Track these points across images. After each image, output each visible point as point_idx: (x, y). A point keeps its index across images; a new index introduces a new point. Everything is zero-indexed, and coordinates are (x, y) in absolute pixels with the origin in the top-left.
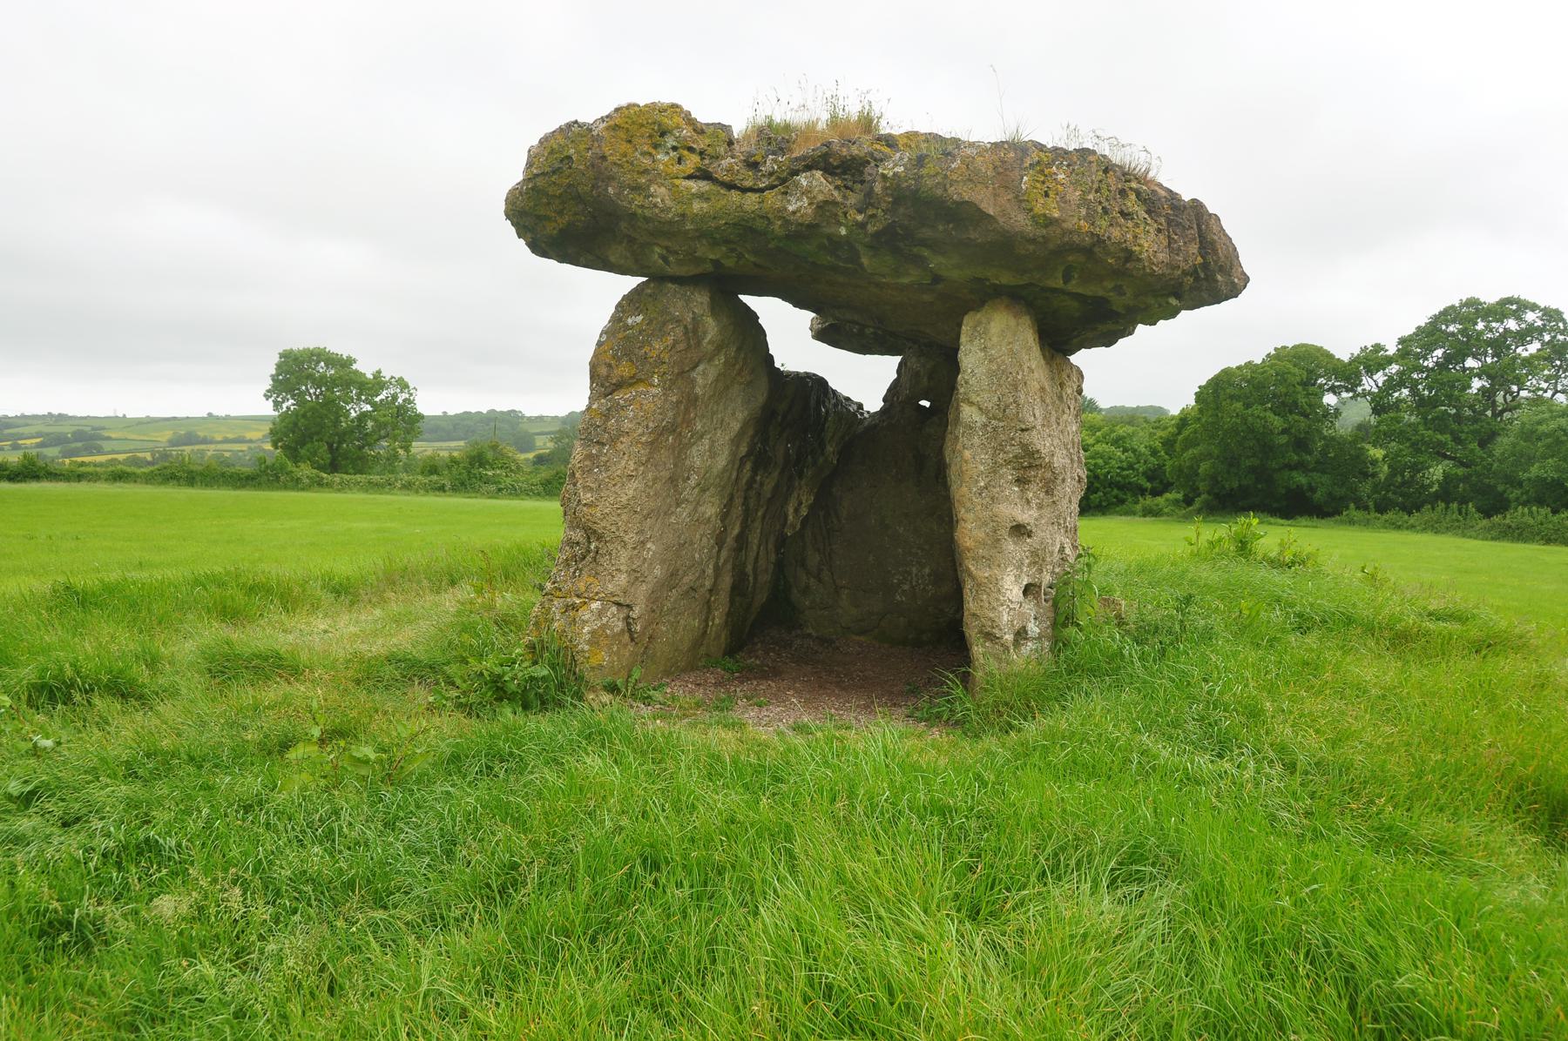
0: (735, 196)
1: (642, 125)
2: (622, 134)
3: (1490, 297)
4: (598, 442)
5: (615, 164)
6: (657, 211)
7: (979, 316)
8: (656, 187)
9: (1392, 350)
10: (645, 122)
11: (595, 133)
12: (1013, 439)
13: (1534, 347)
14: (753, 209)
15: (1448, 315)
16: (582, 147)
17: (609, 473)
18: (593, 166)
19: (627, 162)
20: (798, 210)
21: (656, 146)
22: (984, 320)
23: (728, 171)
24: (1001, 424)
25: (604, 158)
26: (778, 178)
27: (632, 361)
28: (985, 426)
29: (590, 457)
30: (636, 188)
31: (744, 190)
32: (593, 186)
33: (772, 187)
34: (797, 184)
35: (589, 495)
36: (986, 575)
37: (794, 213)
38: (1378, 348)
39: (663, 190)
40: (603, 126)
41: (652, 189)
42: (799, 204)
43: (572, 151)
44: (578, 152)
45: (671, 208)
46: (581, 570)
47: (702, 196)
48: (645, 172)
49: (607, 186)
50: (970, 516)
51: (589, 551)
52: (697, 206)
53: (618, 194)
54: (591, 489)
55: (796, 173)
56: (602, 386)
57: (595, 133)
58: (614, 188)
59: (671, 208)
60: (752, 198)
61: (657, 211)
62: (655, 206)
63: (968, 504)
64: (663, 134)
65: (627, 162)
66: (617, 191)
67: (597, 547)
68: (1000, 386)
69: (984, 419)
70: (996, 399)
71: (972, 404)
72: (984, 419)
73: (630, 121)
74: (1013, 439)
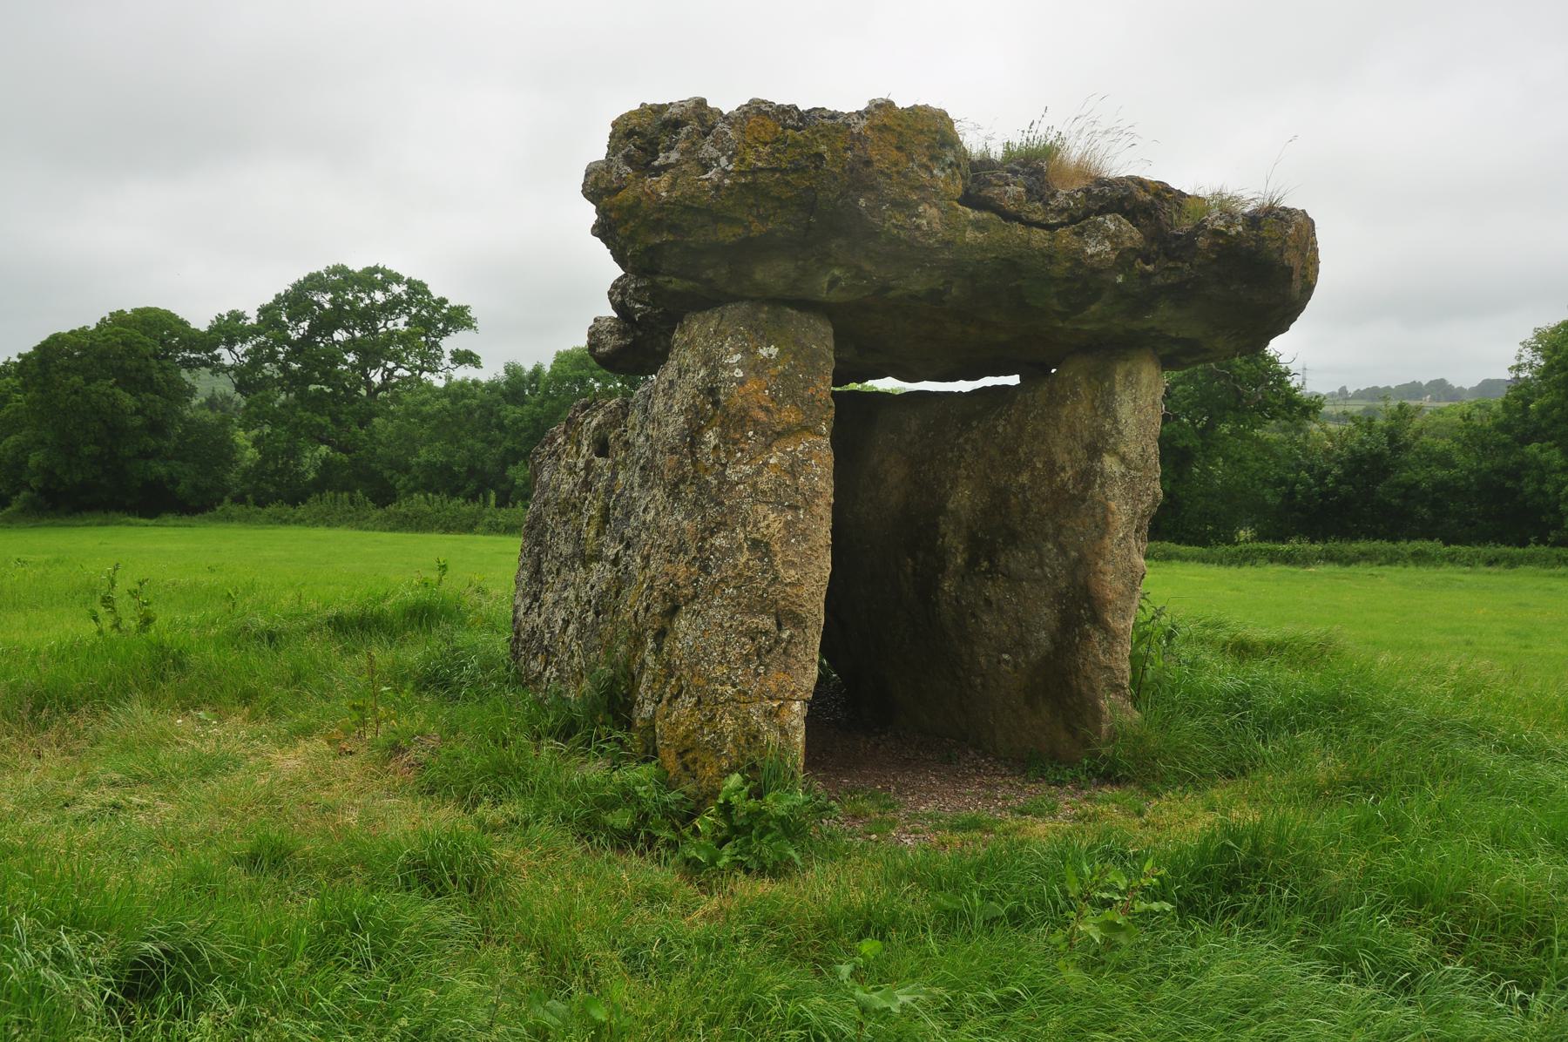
0: (1019, 230)
1: (921, 132)
2: (889, 136)
4: (789, 507)
5: (882, 172)
7: (1129, 365)
8: (927, 206)
10: (926, 129)
11: (855, 131)
12: (1148, 489)
13: (400, 324)
14: (1041, 245)
16: (840, 145)
18: (852, 170)
19: (898, 173)
20: (1098, 254)
21: (933, 158)
23: (1015, 200)
24: (1139, 474)
25: (868, 163)
26: (1071, 216)
27: (796, 405)
28: (1123, 476)
29: (788, 525)
30: (902, 205)
31: (1029, 224)
32: (842, 194)
33: (1061, 225)
34: (1098, 227)
35: (792, 572)
36: (1122, 626)
37: (1092, 256)
38: (236, 316)
39: (934, 211)
40: (863, 123)
41: (921, 209)
42: (1099, 248)
43: (823, 148)
44: (834, 151)
45: (937, 233)
46: (767, 666)
47: (978, 226)
48: (923, 187)
49: (860, 196)
50: (1110, 568)
51: (778, 641)
52: (970, 235)
54: (793, 564)
55: (1102, 211)
57: (855, 131)
58: (868, 199)
59: (937, 233)
60: (1039, 237)
61: (917, 233)
62: (918, 227)
63: (1108, 557)
64: (943, 145)
67: (791, 636)
68: (1145, 436)
70: (1140, 449)
71: (1115, 452)
73: (904, 124)
74: (1148, 489)
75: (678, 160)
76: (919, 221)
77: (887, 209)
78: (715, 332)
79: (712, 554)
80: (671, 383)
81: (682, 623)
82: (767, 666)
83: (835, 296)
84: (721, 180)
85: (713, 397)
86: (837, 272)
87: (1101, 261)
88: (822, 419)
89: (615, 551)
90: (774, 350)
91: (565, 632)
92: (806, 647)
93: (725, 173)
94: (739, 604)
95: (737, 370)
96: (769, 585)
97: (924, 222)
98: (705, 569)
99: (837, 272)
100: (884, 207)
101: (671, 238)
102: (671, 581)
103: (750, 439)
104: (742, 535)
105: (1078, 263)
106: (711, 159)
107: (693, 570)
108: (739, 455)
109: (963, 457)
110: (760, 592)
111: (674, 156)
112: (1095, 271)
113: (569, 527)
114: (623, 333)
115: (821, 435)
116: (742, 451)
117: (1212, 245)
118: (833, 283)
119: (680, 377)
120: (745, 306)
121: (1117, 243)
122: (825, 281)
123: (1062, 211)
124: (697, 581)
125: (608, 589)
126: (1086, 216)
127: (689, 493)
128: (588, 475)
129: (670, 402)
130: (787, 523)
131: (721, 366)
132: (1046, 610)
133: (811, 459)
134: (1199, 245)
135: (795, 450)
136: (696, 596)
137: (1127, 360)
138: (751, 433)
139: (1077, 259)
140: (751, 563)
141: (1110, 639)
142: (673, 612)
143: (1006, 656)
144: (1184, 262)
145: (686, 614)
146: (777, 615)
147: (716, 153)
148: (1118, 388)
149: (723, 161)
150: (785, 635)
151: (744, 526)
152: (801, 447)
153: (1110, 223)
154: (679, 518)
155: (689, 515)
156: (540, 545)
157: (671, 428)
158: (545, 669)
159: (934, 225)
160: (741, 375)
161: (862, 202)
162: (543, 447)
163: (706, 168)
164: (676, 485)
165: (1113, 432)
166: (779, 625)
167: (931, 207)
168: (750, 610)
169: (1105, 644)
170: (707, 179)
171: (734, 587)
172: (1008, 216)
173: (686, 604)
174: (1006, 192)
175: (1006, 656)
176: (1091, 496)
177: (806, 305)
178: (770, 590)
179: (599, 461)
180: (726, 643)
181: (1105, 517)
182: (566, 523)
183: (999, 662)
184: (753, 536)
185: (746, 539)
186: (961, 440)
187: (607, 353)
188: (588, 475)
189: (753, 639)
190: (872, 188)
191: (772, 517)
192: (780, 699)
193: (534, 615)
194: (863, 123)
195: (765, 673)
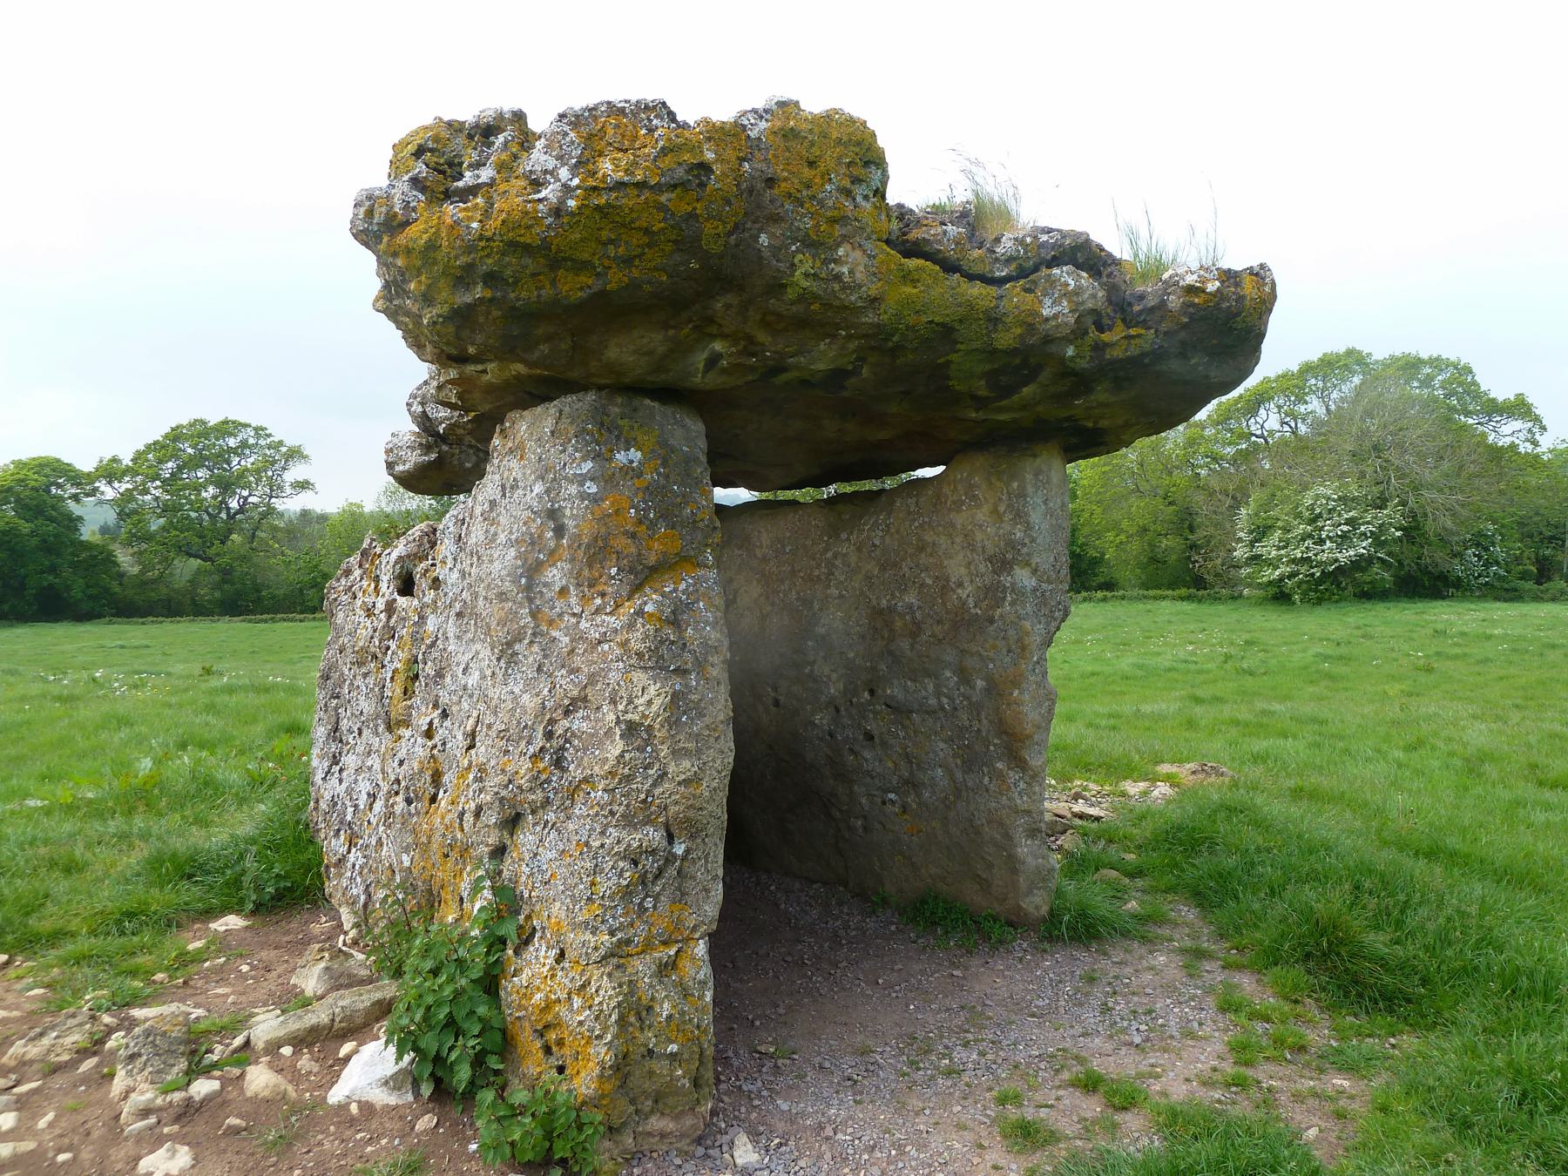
3: (214, 419)
6: (837, 287)
8: (849, 247)
9: (127, 461)
12: (1059, 603)
15: (176, 435)
17: (707, 720)
18: (751, 191)
20: (1055, 316)
22: (1044, 468)
28: (1035, 590)
31: (971, 277)
32: (736, 226)
34: (1052, 282)
35: (686, 764)
37: (1047, 320)
41: (841, 252)
45: (860, 286)
46: (656, 898)
49: (761, 230)
53: (775, 250)
54: (686, 753)
56: (631, 571)
58: (772, 236)
59: (860, 286)
61: (837, 287)
62: (838, 277)
64: (867, 164)
65: (813, 197)
66: (776, 243)
67: (687, 851)
69: (1034, 582)
70: (1052, 559)
72: (1034, 582)
75: (493, 179)
76: (838, 269)
77: (798, 251)
78: (552, 433)
79: (567, 741)
80: (493, 504)
81: (526, 838)
82: (656, 898)
83: (713, 381)
84: (562, 201)
85: (553, 519)
86: (718, 346)
87: (1058, 326)
88: (706, 545)
89: (428, 720)
90: (635, 455)
91: (371, 809)
92: (707, 861)
93: (567, 189)
94: (612, 813)
95: (588, 484)
96: (654, 785)
97: (845, 270)
98: (558, 763)
99: (718, 346)
100: (794, 248)
101: (488, 294)
102: (510, 781)
103: (613, 578)
104: (612, 717)
105: (1030, 328)
106: (546, 172)
107: (542, 765)
108: (598, 601)
109: (833, 574)
110: (643, 796)
111: (486, 174)
112: (1048, 340)
113: (371, 680)
114: (427, 448)
115: (706, 566)
116: (603, 595)
117: (1186, 305)
118: (712, 362)
119: (504, 495)
120: (591, 397)
121: (1078, 304)
122: (700, 358)
123: (1009, 260)
124: (548, 781)
125: (421, 771)
126: (1036, 269)
127: (530, 655)
128: (389, 617)
129: (493, 529)
130: (675, 695)
131: (566, 478)
132: (942, 745)
133: (697, 601)
134: (1171, 306)
135: (675, 590)
136: (547, 802)
137: (1035, 456)
138: (614, 571)
139: (1030, 323)
140: (627, 756)
141: (1027, 778)
142: (512, 822)
143: (892, 796)
144: (1149, 328)
145: (534, 825)
146: (667, 827)
147: (552, 163)
148: (1030, 490)
149: (564, 173)
150: (679, 849)
151: (613, 702)
152: (683, 586)
153: (1066, 276)
154: (517, 690)
155: (529, 685)
156: (338, 697)
157: (497, 565)
158: (349, 852)
159: (858, 275)
160: (594, 489)
161: (764, 239)
162: (338, 580)
163: (537, 184)
164: (509, 644)
165: (1026, 541)
166: (670, 838)
167: (854, 249)
168: (628, 822)
169: (1022, 785)
170: (540, 200)
171: (605, 790)
172: (949, 267)
173: (533, 812)
174: (945, 232)
175: (892, 796)
176: (1001, 616)
177: (671, 394)
178: (657, 791)
179: (402, 601)
180: (596, 870)
181: (1019, 640)
182: (365, 675)
183: (884, 803)
184: (629, 717)
185: (618, 722)
186: (829, 555)
187: (408, 471)
188: (389, 617)
189: (635, 863)
190: (776, 219)
191: (652, 690)
192: (677, 942)
193: (334, 781)
194: (763, 125)
195: (655, 907)
